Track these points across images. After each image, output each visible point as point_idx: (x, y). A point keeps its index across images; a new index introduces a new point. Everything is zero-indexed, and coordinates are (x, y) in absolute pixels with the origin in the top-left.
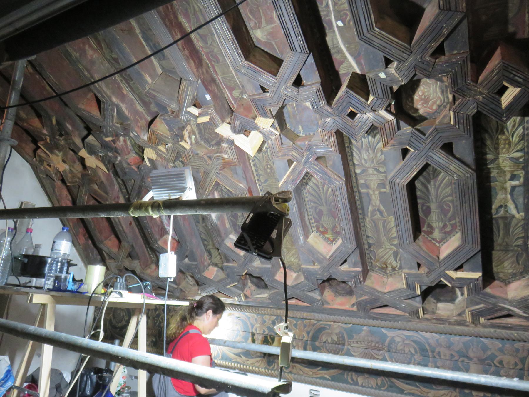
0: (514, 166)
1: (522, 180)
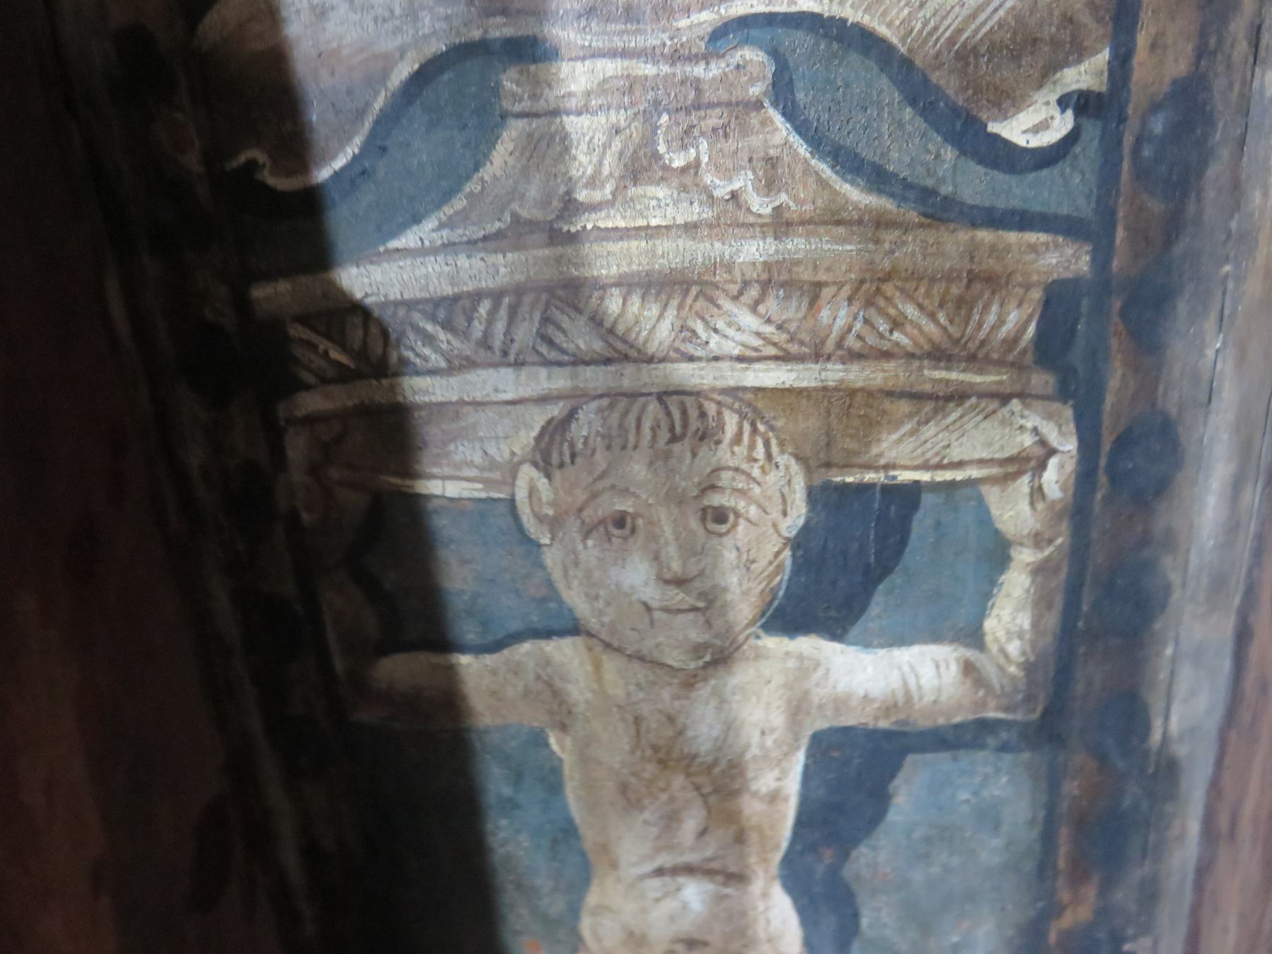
0: (871, 288)
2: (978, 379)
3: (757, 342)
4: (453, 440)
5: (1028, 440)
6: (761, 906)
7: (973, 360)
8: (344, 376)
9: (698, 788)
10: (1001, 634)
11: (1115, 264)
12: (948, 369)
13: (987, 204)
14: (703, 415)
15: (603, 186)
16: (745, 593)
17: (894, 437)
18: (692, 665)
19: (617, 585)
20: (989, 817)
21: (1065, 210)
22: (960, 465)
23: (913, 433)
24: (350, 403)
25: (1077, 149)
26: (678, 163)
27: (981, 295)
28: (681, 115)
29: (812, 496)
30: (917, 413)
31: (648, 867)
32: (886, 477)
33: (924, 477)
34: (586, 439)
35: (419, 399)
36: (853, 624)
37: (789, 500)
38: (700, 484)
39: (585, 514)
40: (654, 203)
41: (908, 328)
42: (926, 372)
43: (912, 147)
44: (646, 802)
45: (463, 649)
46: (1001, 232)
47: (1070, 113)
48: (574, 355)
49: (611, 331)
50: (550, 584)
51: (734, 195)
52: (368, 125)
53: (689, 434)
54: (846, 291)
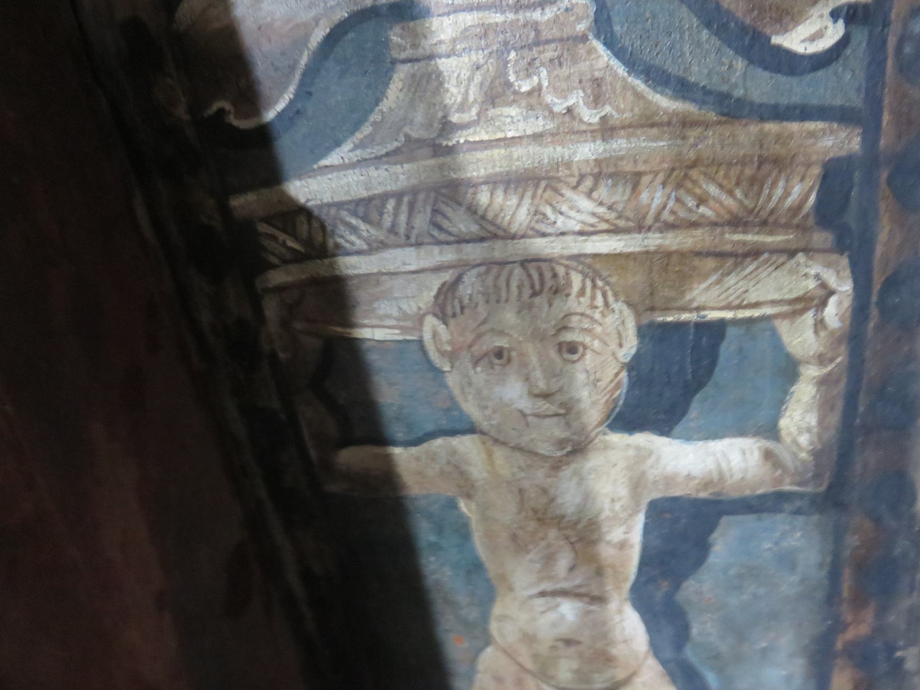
0: (680, 174)
1: (802, 419)
2: (769, 239)
3: (593, 220)
4: (377, 299)
5: (811, 284)
6: (617, 618)
7: (764, 225)
8: (298, 258)
9: (567, 538)
10: (793, 430)
11: (882, 142)
12: (745, 232)
13: (773, 102)
14: (555, 276)
15: (470, 108)
16: (594, 403)
17: (704, 286)
18: (559, 454)
19: (501, 399)
20: (787, 560)
21: (838, 102)
22: (757, 305)
23: (718, 282)
24: (303, 277)
25: (848, 51)
26: (525, 87)
27: (769, 175)
28: (526, 52)
29: (642, 332)
30: (721, 267)
31: (535, 591)
32: (698, 317)
33: (728, 315)
34: (471, 295)
35: (350, 272)
36: (676, 424)
37: (624, 335)
38: (555, 325)
39: (474, 348)
40: (508, 120)
41: (712, 203)
42: (727, 236)
43: (708, 60)
44: (531, 547)
45: (395, 443)
46: (785, 123)
47: (841, 23)
48: (458, 236)
49: (483, 217)
50: (452, 398)
51: (569, 110)
52: (297, 76)
53: (546, 289)
54: (661, 177)
